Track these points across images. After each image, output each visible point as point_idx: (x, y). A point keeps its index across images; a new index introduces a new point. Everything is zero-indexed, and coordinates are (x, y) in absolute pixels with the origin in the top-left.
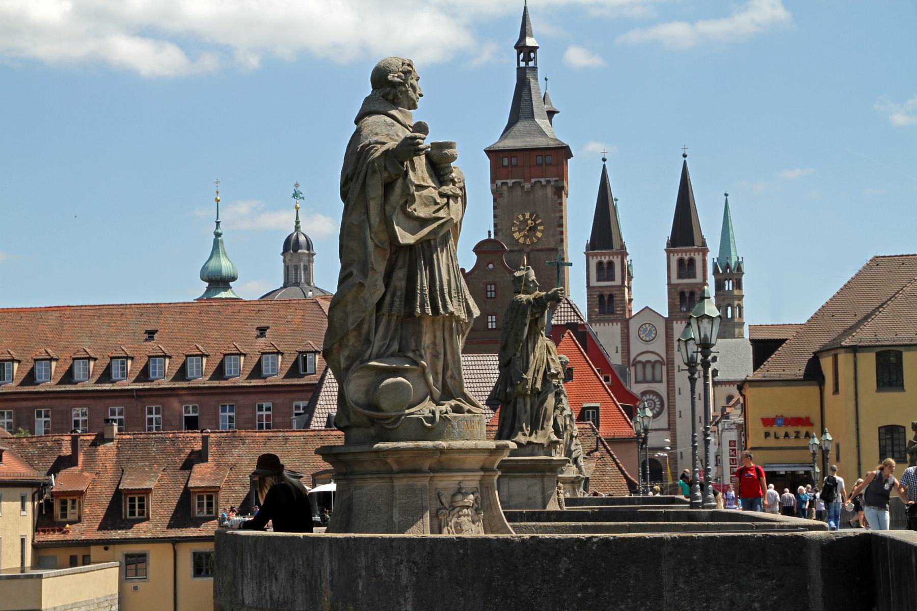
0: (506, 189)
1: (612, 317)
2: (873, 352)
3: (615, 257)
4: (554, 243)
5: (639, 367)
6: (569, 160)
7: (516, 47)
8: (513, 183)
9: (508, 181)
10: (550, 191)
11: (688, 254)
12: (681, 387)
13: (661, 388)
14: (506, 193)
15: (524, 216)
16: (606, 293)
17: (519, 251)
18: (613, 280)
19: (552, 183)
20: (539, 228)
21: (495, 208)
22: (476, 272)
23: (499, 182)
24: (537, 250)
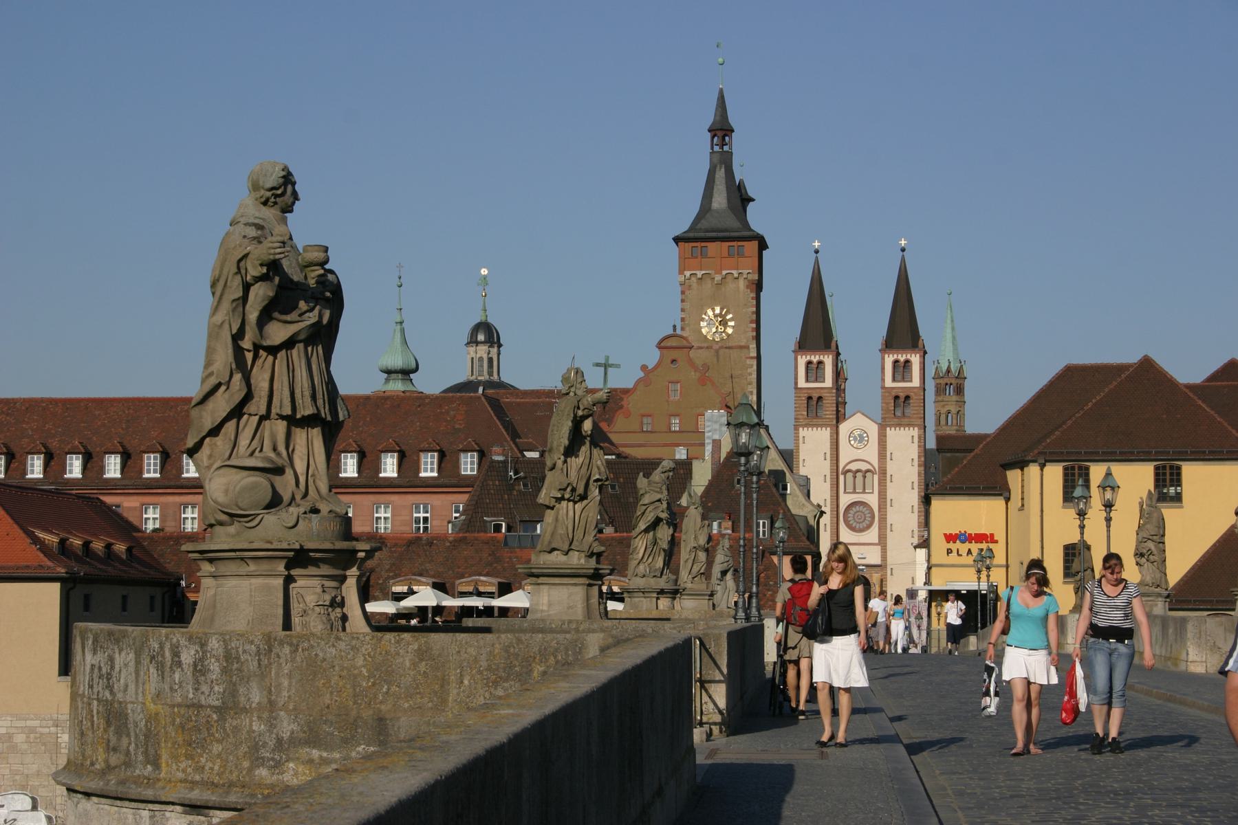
0: (695, 281)
1: (820, 421)
2: (1060, 466)
3: (826, 356)
4: (745, 341)
5: (850, 475)
7: (709, 131)
9: (698, 272)
10: (742, 284)
11: (904, 355)
12: (893, 498)
13: (872, 500)
15: (713, 310)
16: (815, 396)
17: (707, 348)
18: (824, 381)
20: (730, 324)
21: (683, 301)
22: (659, 370)
23: (688, 273)
24: (726, 348)
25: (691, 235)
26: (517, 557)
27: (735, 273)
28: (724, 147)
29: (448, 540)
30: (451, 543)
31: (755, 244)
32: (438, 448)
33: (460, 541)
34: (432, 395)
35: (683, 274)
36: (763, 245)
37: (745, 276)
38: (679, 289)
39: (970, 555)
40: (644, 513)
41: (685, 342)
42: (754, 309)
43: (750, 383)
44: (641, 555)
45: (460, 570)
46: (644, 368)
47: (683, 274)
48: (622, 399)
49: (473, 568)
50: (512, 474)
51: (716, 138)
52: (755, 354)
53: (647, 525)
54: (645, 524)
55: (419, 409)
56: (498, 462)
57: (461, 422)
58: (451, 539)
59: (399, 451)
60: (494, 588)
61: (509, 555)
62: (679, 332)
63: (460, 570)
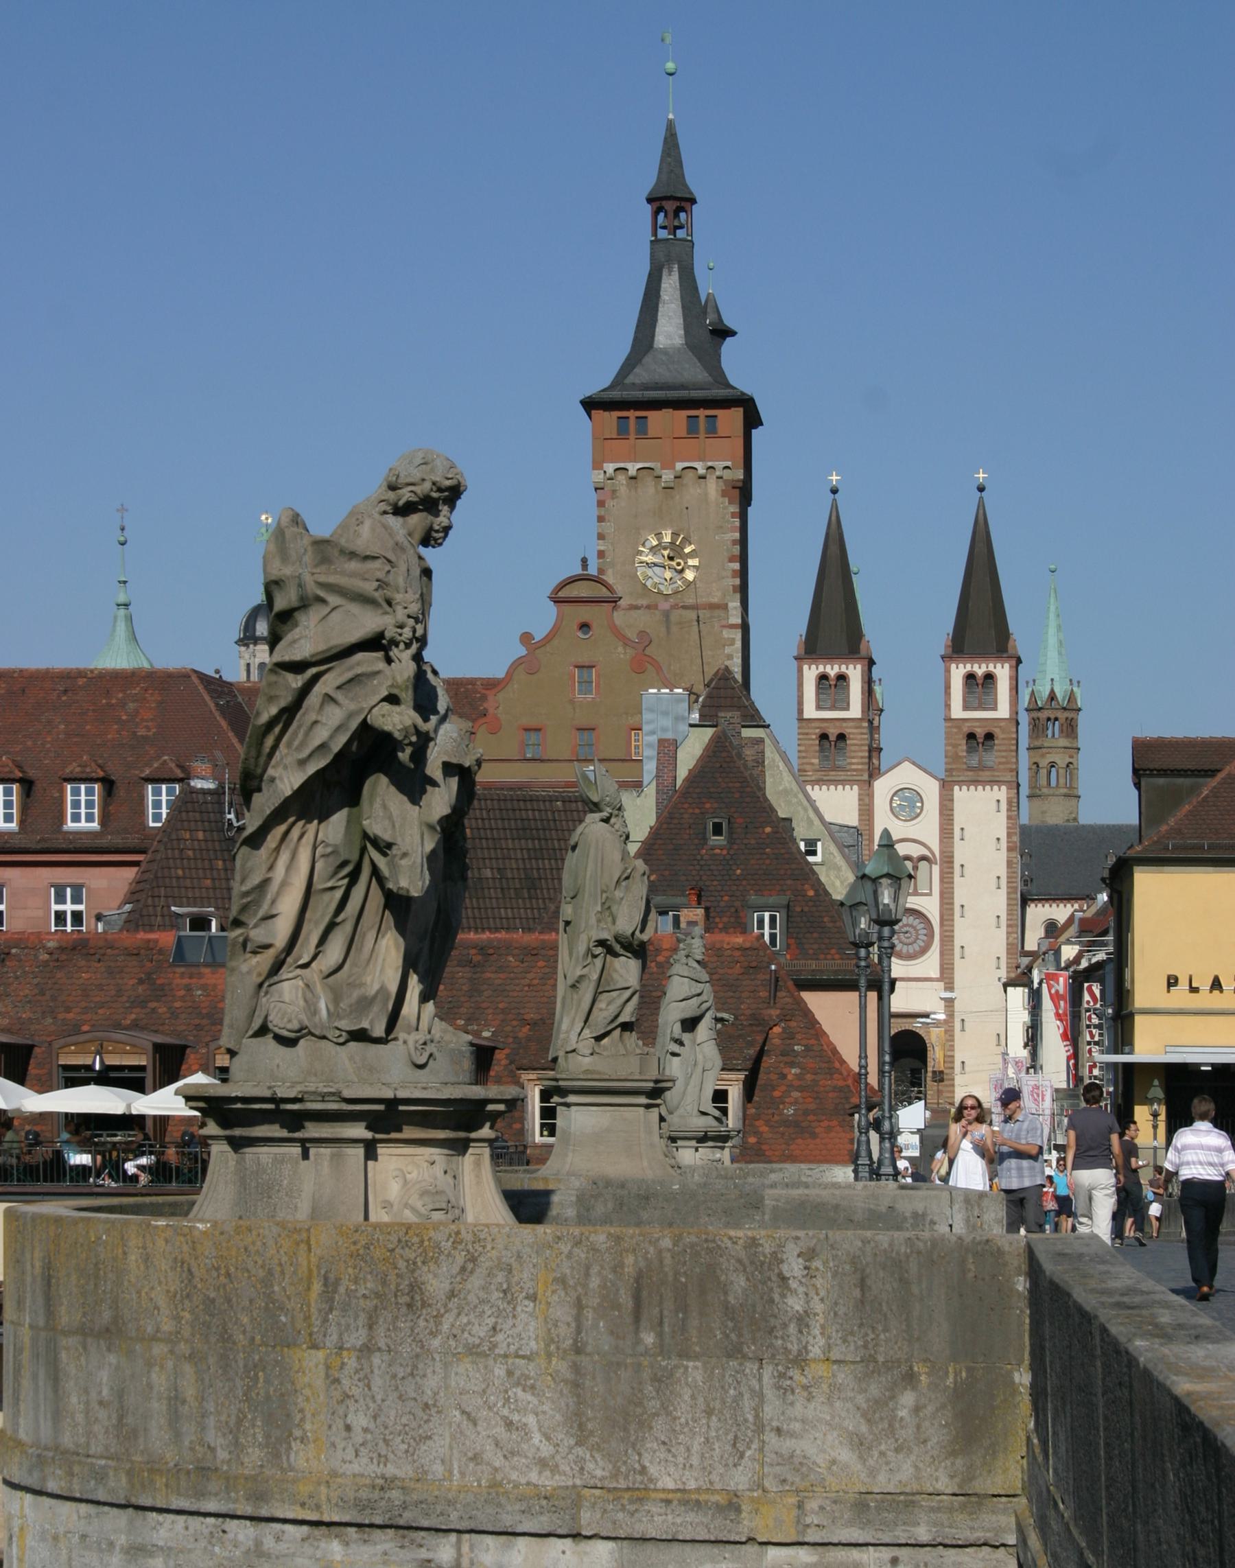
4: (719, 594)
9: (629, 466)
10: (713, 488)
14: (623, 490)
15: (659, 535)
17: (648, 607)
20: (691, 562)
21: (601, 519)
22: (555, 642)
23: (610, 468)
24: (684, 607)
25: (616, 395)
26: (204, 987)
27: (701, 468)
28: (678, 232)
29: (44, 947)
30: (51, 954)
31: (737, 414)
32: (101, 774)
33: (74, 949)
34: (92, 671)
35: (601, 468)
36: (752, 419)
37: (718, 473)
38: (594, 497)
39: (1216, 992)
40: (289, 713)
41: (604, 589)
42: (737, 535)
44: (281, 930)
45: (71, 1016)
46: (526, 638)
47: (601, 468)
48: (484, 698)
49: (100, 1011)
50: (232, 816)
51: (661, 216)
52: (739, 621)
53: (312, 769)
54: (302, 763)
55: (64, 698)
56: (204, 792)
57: (150, 724)
58: (51, 944)
59: (20, 781)
60: (144, 1057)
61: (186, 981)
62: (592, 570)
63: (71, 1016)
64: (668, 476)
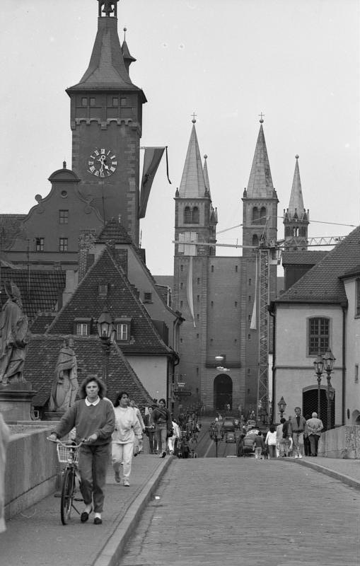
3: (200, 204)
6: (143, 105)
8: (91, 121)
10: (123, 131)
18: (198, 223)
19: (126, 123)
20: (113, 163)
36: (143, 99)
37: (126, 123)
43: (130, 213)
46: (38, 197)
64: (103, 125)
